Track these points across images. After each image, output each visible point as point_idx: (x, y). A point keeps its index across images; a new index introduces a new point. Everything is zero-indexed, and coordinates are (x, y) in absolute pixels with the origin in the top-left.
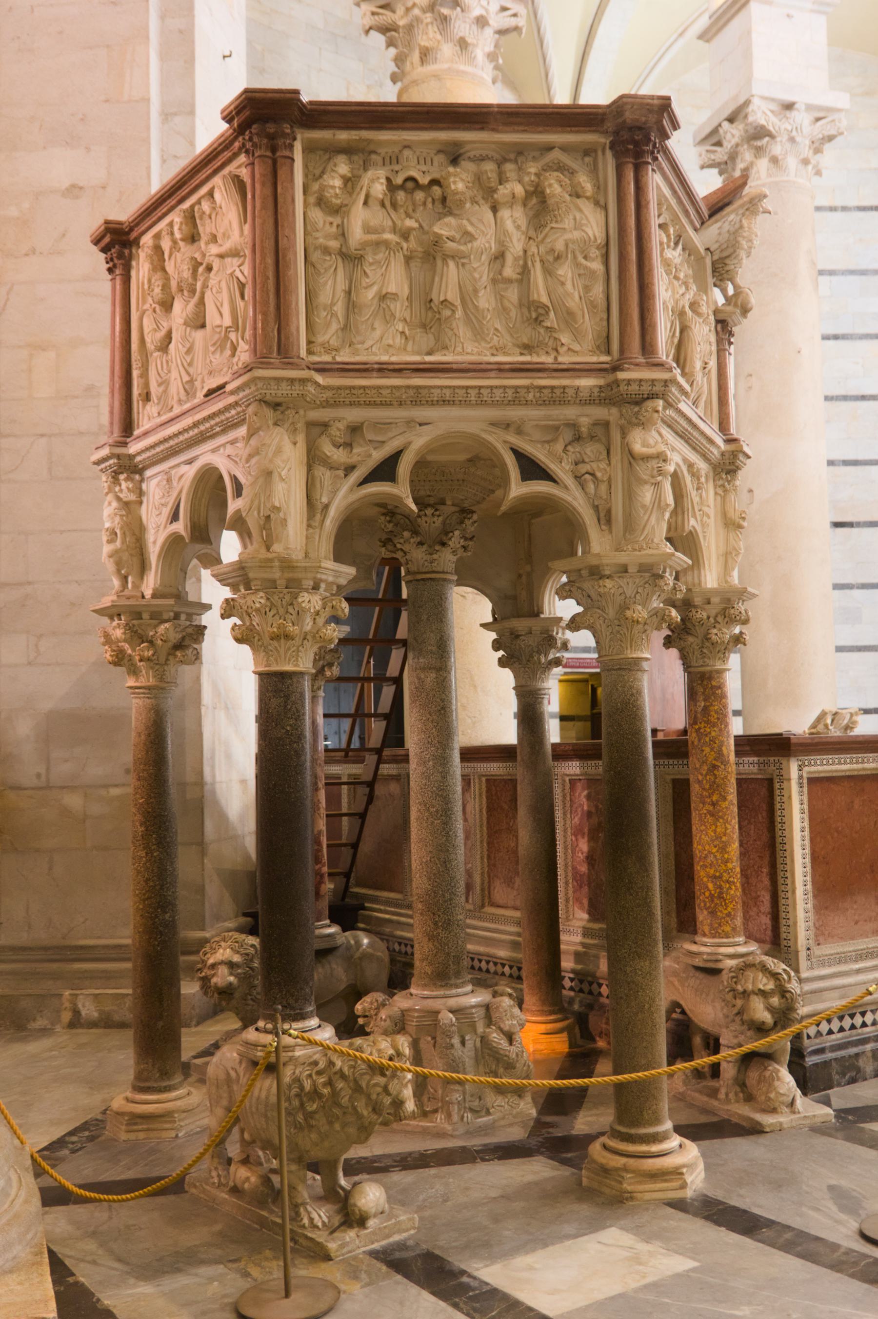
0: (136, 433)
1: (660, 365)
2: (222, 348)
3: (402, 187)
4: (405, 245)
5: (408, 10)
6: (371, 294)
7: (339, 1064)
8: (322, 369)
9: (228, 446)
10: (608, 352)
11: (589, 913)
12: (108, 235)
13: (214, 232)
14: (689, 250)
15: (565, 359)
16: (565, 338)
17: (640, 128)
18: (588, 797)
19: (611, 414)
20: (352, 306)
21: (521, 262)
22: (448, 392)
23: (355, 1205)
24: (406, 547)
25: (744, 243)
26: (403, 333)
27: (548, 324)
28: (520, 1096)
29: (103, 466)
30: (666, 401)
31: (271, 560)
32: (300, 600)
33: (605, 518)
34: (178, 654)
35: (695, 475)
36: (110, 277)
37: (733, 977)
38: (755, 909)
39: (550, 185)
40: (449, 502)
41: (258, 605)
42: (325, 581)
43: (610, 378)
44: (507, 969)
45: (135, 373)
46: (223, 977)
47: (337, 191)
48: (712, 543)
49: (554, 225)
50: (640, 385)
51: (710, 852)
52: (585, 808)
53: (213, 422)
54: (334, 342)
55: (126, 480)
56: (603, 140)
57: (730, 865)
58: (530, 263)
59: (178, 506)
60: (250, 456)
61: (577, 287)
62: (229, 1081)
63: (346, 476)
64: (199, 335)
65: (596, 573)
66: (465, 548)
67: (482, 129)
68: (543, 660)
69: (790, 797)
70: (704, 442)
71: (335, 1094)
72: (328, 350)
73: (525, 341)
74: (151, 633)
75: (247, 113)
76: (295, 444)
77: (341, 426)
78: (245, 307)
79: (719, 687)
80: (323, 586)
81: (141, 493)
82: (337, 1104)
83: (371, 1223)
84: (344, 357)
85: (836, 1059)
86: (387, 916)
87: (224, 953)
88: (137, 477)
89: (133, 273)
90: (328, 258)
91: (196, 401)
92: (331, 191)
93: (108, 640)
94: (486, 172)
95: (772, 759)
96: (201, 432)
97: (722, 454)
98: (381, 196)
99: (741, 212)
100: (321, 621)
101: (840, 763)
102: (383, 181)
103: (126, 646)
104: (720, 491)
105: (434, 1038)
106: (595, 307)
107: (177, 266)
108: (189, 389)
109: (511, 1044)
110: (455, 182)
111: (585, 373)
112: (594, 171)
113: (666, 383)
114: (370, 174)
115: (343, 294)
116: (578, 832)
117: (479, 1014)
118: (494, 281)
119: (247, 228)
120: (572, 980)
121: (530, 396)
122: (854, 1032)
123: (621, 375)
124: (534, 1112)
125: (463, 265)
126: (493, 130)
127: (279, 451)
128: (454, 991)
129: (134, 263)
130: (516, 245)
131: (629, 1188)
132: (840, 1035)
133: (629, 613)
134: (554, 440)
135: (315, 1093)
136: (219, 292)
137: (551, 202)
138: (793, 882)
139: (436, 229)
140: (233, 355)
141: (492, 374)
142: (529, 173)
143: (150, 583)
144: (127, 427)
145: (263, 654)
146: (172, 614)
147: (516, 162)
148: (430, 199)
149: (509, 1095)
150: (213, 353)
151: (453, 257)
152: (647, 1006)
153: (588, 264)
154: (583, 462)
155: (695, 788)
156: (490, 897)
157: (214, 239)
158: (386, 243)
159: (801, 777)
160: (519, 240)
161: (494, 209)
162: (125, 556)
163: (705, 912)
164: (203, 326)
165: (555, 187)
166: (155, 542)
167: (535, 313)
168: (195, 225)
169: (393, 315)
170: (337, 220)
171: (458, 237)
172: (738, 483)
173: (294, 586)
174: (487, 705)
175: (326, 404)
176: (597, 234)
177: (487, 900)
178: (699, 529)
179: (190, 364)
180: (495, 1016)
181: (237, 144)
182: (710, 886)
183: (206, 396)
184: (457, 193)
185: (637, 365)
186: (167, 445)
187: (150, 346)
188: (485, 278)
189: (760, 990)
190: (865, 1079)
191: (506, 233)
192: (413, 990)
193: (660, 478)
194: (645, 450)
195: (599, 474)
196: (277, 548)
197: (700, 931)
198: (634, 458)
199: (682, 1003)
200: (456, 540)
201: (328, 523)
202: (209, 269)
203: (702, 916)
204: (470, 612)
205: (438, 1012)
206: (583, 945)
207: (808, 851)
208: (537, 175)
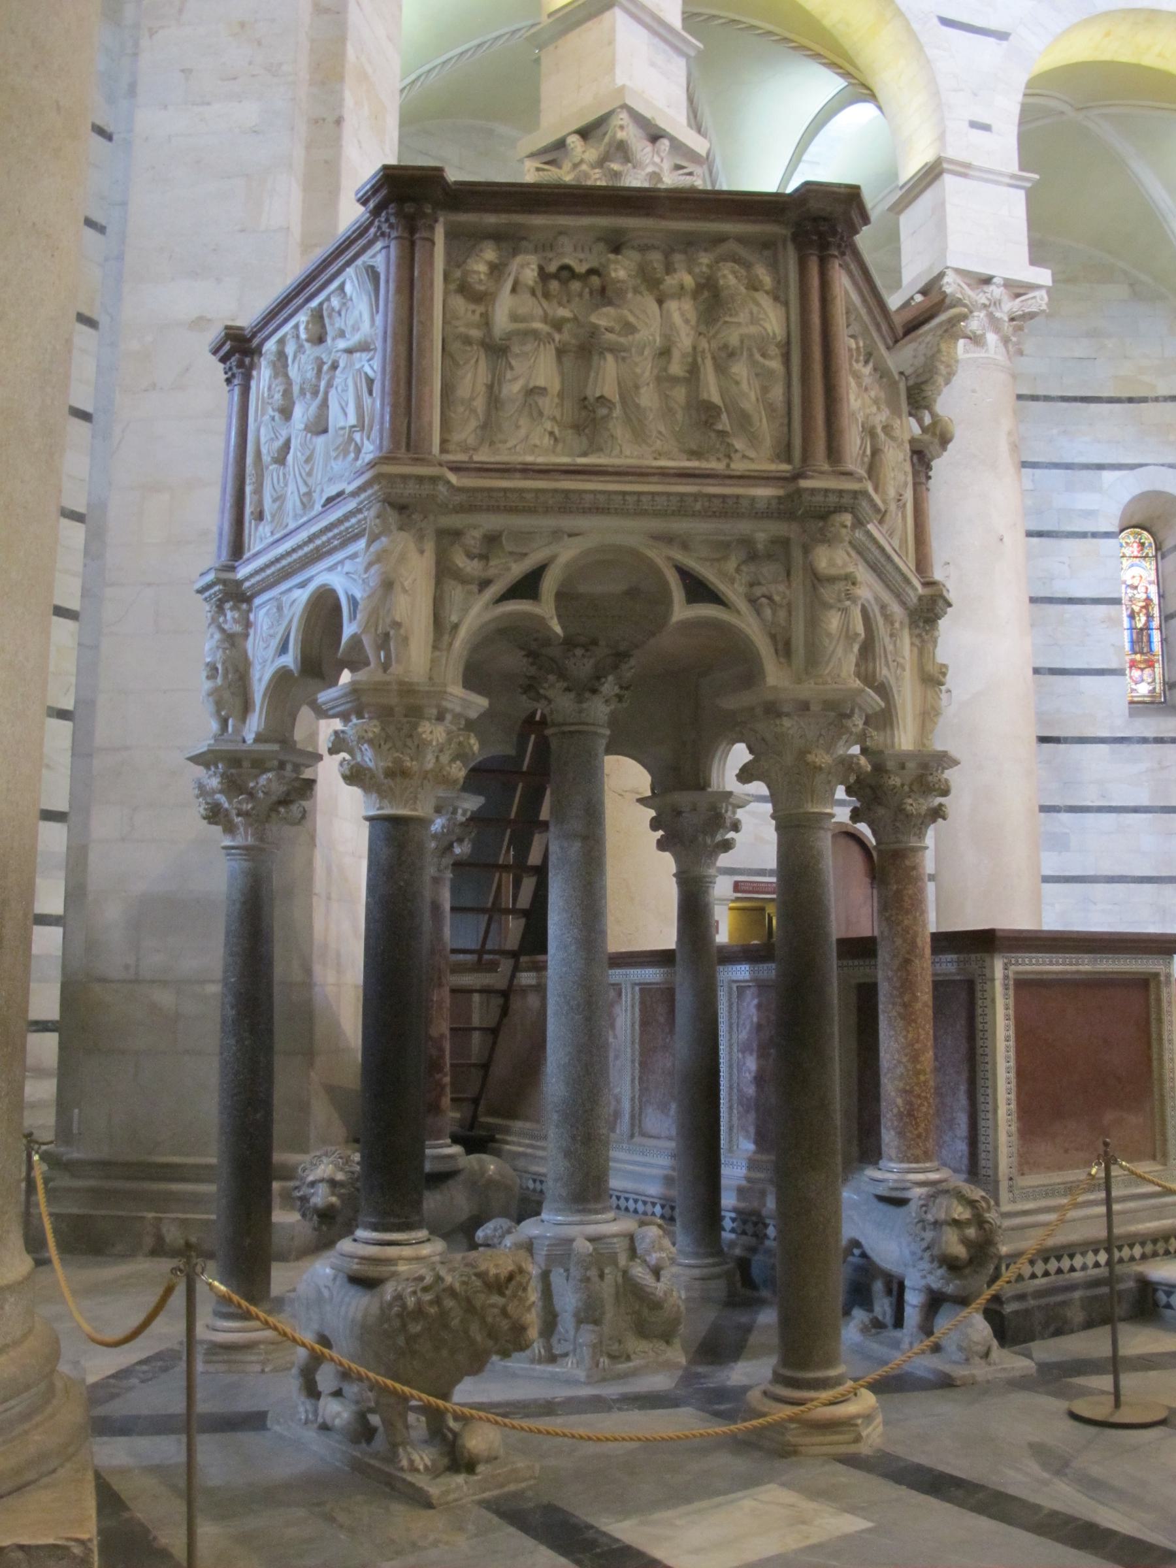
0: (246, 556)
1: (849, 474)
2: (346, 453)
3: (555, 276)
4: (557, 337)
5: (575, 166)
6: (516, 387)
7: (449, 1279)
8: (456, 468)
9: (348, 562)
10: (789, 460)
11: (756, 1143)
12: (229, 343)
13: (343, 327)
14: (881, 372)
15: (739, 466)
16: (739, 444)
17: (825, 219)
18: (759, 1007)
19: (790, 530)
20: (494, 400)
21: (690, 360)
22: (601, 498)
23: (464, 1446)
24: (550, 693)
25: (942, 368)
26: (551, 433)
27: (720, 427)
28: (668, 1342)
29: (207, 594)
30: (855, 516)
31: (388, 683)
32: (420, 730)
33: (784, 649)
34: (282, 810)
35: (889, 619)
36: (228, 388)
37: (923, 1206)
38: (950, 1134)
39: (724, 276)
40: (602, 643)
41: (371, 735)
42: (452, 711)
43: (791, 487)
44: (658, 1209)
45: (248, 489)
46: (321, 1197)
47: (482, 277)
48: (907, 696)
49: (728, 319)
50: (826, 496)
51: (900, 1062)
52: (755, 1019)
53: (330, 534)
54: (471, 441)
55: (232, 609)
56: (784, 232)
57: (922, 1078)
58: (699, 360)
59: (288, 635)
60: (370, 565)
61: (753, 388)
62: (320, 1300)
63: (480, 591)
64: (320, 441)
65: (772, 710)
66: (620, 698)
67: (648, 215)
68: (709, 841)
69: (993, 1001)
70: (899, 579)
71: (444, 1314)
72: (466, 449)
73: (695, 448)
74: (252, 785)
75: (384, 192)
76: (422, 552)
77: (477, 534)
78: (375, 404)
79: (914, 868)
80: (449, 717)
81: (248, 624)
82: (446, 1326)
83: (480, 1468)
84: (483, 456)
85: (1039, 1307)
86: (521, 1149)
87: (325, 1169)
88: (244, 606)
89: (253, 384)
90: (468, 348)
91: (314, 513)
92: (475, 276)
93: (202, 791)
94: (651, 261)
95: (973, 956)
96: (317, 548)
97: (920, 598)
98: (531, 283)
99: (940, 332)
100: (445, 759)
101: (1051, 964)
102: (534, 267)
103: (222, 799)
104: (917, 642)
105: (567, 1270)
106: (773, 410)
107: (300, 370)
108: (306, 500)
109: (658, 1280)
110: (615, 270)
111: (763, 482)
112: (774, 266)
113: (855, 494)
114: (519, 259)
115: (484, 389)
116: (745, 1049)
117: (621, 1246)
118: (659, 379)
119: (379, 319)
120: (733, 1220)
121: (698, 506)
122: (1061, 1277)
123: (804, 484)
124: (683, 1360)
125: (624, 359)
126: (662, 217)
127: (402, 558)
128: (593, 1217)
129: (255, 373)
130: (685, 340)
131: (793, 1440)
132: (1044, 1280)
133: (810, 758)
134: (725, 558)
135: (419, 1312)
136: (345, 390)
137: (724, 294)
138: (995, 1100)
139: (594, 319)
140: (356, 458)
141: (655, 479)
142: (701, 264)
143: (254, 724)
144: (237, 549)
145: (374, 795)
146: (276, 763)
147: (686, 252)
148: (587, 290)
149: (655, 1340)
150: (336, 458)
151: (611, 350)
153: (767, 363)
154: (759, 584)
155: (884, 989)
156: (640, 1127)
157: (342, 334)
158: (535, 334)
159: (1006, 977)
160: (688, 335)
161: (660, 302)
162: (227, 695)
163: (892, 1133)
164: (325, 431)
165: (730, 278)
166: (260, 680)
167: (705, 414)
168: (323, 326)
169: (541, 414)
170: (480, 309)
171: (617, 328)
172: (936, 633)
173: (415, 713)
174: (642, 898)
175: (460, 509)
176: (777, 331)
177: (637, 1129)
178: (893, 682)
179: (309, 474)
180: (641, 1248)
181: (372, 230)
182: (899, 1101)
183: (323, 506)
184: (619, 281)
185: (822, 473)
186: (278, 566)
187: (266, 459)
188: (647, 374)
190: (1072, 1332)
191: (672, 326)
192: (544, 1216)
193: (848, 603)
194: (833, 571)
195: (777, 598)
196: (396, 669)
197: (884, 1155)
198: (819, 580)
199: (863, 1241)
200: (609, 687)
201: (457, 644)
202: (334, 366)
203: (889, 1137)
204: (626, 780)
205: (572, 1241)
206: (748, 1179)
207: (1012, 1064)
208: (710, 266)
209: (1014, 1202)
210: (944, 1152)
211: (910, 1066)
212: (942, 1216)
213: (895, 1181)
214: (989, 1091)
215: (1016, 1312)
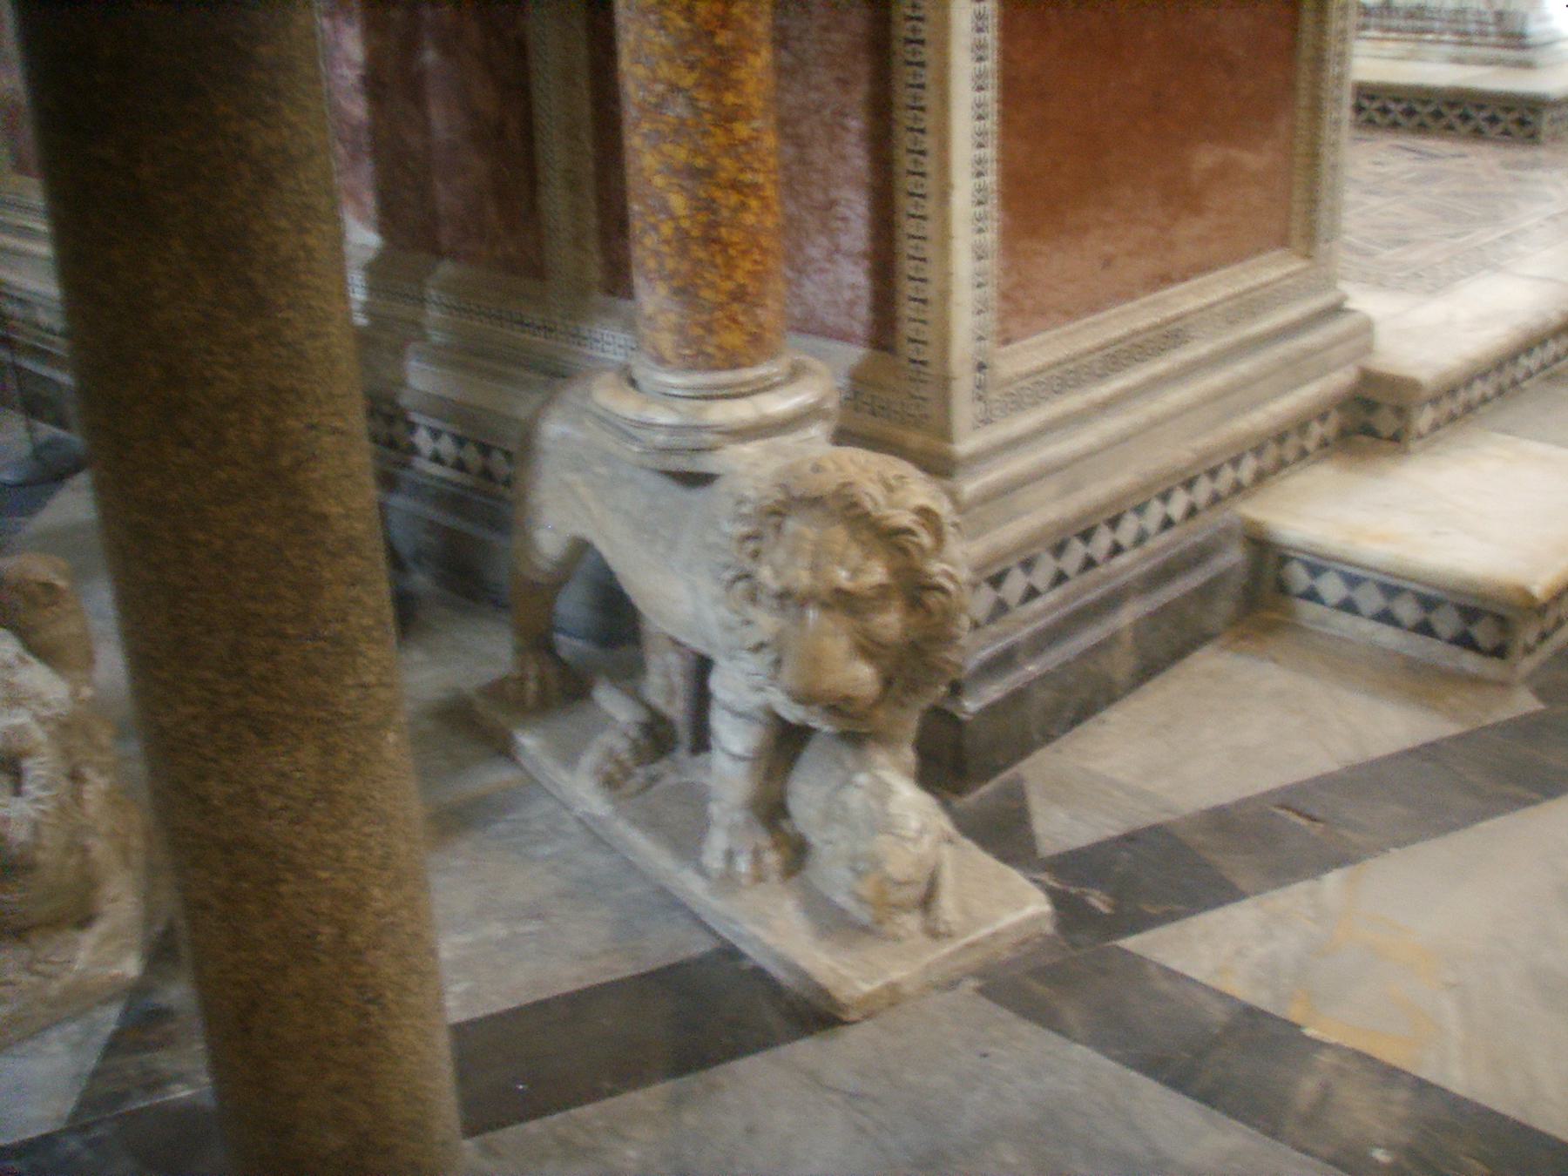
37: (748, 538)
38: (823, 241)
51: (674, 88)
57: (742, 130)
152: (327, 933)
163: (662, 290)
182: (678, 202)
189: (839, 591)
207: (991, 64)
209: (986, 422)
210: (809, 288)
211: (704, 99)
212: (802, 578)
213: (673, 429)
214: (928, 142)
215: (991, 710)
